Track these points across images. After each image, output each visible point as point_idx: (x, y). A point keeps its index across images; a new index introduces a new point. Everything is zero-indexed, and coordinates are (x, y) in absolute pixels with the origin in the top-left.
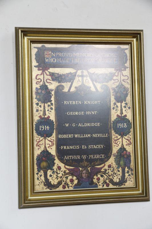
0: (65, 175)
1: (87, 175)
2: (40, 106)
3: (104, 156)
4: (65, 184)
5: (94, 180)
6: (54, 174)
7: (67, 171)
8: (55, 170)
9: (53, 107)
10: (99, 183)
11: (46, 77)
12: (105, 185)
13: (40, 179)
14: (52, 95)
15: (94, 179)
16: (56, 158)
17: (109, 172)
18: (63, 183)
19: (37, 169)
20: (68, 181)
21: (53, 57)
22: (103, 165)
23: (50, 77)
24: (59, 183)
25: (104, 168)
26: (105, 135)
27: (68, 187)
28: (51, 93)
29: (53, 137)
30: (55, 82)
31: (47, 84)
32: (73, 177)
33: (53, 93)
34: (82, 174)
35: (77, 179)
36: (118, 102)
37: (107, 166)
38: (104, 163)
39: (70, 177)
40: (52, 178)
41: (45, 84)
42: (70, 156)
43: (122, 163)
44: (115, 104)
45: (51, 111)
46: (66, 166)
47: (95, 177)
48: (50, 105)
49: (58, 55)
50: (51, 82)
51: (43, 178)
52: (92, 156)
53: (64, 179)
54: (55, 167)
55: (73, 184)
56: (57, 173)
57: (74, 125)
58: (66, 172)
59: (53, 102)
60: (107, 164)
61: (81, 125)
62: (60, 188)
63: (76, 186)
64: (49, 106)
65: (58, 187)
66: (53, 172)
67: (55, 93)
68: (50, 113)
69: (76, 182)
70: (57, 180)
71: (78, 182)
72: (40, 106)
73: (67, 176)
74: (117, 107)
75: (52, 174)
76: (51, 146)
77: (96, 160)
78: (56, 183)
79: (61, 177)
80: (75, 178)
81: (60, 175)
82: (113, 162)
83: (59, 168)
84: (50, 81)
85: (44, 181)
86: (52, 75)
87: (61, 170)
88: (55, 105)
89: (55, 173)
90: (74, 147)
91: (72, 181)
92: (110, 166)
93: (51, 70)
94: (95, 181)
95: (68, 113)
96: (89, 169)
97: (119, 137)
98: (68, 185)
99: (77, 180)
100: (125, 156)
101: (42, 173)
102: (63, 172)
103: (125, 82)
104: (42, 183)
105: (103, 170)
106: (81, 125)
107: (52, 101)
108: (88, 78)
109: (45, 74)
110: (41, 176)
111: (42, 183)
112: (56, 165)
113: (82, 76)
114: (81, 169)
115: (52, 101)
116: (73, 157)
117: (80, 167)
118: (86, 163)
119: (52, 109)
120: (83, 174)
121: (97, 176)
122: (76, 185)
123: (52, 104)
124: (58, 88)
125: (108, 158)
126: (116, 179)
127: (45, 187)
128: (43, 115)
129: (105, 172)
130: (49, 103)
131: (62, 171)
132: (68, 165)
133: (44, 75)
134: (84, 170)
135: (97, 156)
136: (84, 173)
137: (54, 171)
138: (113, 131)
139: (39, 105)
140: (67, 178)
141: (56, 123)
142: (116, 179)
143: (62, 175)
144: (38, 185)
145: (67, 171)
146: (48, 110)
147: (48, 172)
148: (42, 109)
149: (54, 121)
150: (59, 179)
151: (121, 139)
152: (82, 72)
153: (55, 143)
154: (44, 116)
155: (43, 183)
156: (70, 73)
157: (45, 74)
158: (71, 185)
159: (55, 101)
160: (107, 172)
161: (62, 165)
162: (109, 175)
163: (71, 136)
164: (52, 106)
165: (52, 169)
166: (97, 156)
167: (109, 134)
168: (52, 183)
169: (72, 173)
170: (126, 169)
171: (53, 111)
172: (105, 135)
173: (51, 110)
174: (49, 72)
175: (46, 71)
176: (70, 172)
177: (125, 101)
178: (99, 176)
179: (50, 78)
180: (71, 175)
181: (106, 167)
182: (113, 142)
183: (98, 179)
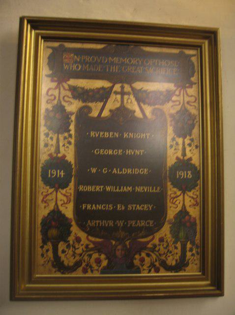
0: (87, 251)
1: (123, 252)
2: (52, 139)
3: (154, 223)
4: (87, 265)
5: (134, 261)
6: (69, 249)
7: (91, 246)
8: (71, 242)
9: (73, 141)
10: (142, 266)
11: (63, 93)
12: (153, 270)
13: (45, 256)
14: (72, 121)
15: (135, 259)
16: (73, 223)
17: (159, 250)
18: (84, 264)
19: (42, 239)
20: (92, 260)
21: (76, 62)
22: (151, 237)
23: (70, 93)
24: (78, 264)
25: (152, 243)
26: (156, 189)
27: (92, 271)
28: (70, 118)
29: (70, 189)
30: (77, 100)
31: (64, 103)
32: (100, 255)
33: (73, 118)
34: (115, 250)
35: (107, 258)
36: (179, 136)
37: (158, 239)
38: (153, 234)
39: (95, 256)
40: (66, 255)
41: (61, 102)
42: (97, 222)
43: (182, 234)
44: (173, 139)
45: (67, 147)
46: (90, 238)
47: (137, 256)
48: (68, 137)
49: (84, 60)
50: (72, 100)
51: (50, 254)
52: (133, 222)
53: (86, 258)
54: (71, 239)
55: (100, 266)
56: (74, 247)
57: (105, 171)
58: (90, 246)
59: (73, 132)
60: (158, 236)
61: (117, 171)
62: (79, 274)
63: (105, 270)
64: (65, 138)
65: (75, 270)
66: (68, 246)
67: (77, 118)
68: (67, 149)
69: (105, 263)
70: (74, 258)
71: (108, 264)
72: (52, 139)
73: (91, 252)
74: (177, 144)
75: (65, 249)
76: (67, 203)
77: (140, 229)
78: (71, 264)
79: (81, 255)
80: (103, 256)
81: (79, 251)
82: (168, 233)
83: (78, 240)
84: (70, 100)
85: (52, 259)
86: (73, 89)
87: (82, 243)
88: (75, 137)
89: (71, 248)
90: (104, 207)
91: (98, 261)
92: (161, 240)
93: (72, 82)
94: (137, 262)
95: (97, 151)
96: (127, 243)
97: (179, 193)
98: (91, 267)
99: (107, 261)
100: (188, 224)
101: (49, 246)
102: (83, 247)
103: (191, 105)
104: (48, 262)
105: (150, 246)
106: (117, 171)
107: (70, 130)
108: (132, 97)
109: (62, 88)
110: (47, 251)
111: (48, 262)
112: (73, 234)
113: (123, 93)
114: (114, 243)
115: (70, 130)
116: (102, 222)
117: (114, 240)
118: (122, 234)
119: (70, 143)
120: (116, 252)
121: (140, 255)
122: (105, 268)
123: (70, 136)
124: (81, 110)
125: (159, 226)
126: (171, 261)
127: (54, 270)
128: (55, 152)
129: (153, 249)
130: (66, 134)
131: (82, 245)
132: (93, 236)
133: (60, 89)
134: (120, 244)
135: (142, 223)
136: (118, 250)
137: (69, 244)
138: (169, 184)
139: (50, 136)
140: (90, 256)
141: (76, 166)
142: (171, 261)
143: (82, 252)
144: (43, 265)
145: (91, 246)
146: (64, 145)
147: (60, 245)
148: (54, 142)
149: (73, 162)
150: (78, 258)
151: (182, 196)
152: (122, 87)
153: (72, 198)
154: (57, 154)
155: (50, 264)
156: (103, 88)
157: (62, 88)
158: (96, 268)
159: (76, 131)
160: (157, 249)
161: (83, 235)
162: (160, 255)
163: (100, 189)
164: (70, 139)
165: (66, 241)
166: (142, 223)
167: (162, 187)
168: (66, 263)
169: (98, 248)
170: (189, 246)
171: (72, 147)
172: (156, 189)
173: (68, 145)
174: (69, 85)
175: (64, 84)
176: (96, 247)
177: (190, 136)
178: (143, 255)
179: (69, 94)
180: (97, 252)
181: (156, 241)
182: (168, 201)
183: (142, 260)
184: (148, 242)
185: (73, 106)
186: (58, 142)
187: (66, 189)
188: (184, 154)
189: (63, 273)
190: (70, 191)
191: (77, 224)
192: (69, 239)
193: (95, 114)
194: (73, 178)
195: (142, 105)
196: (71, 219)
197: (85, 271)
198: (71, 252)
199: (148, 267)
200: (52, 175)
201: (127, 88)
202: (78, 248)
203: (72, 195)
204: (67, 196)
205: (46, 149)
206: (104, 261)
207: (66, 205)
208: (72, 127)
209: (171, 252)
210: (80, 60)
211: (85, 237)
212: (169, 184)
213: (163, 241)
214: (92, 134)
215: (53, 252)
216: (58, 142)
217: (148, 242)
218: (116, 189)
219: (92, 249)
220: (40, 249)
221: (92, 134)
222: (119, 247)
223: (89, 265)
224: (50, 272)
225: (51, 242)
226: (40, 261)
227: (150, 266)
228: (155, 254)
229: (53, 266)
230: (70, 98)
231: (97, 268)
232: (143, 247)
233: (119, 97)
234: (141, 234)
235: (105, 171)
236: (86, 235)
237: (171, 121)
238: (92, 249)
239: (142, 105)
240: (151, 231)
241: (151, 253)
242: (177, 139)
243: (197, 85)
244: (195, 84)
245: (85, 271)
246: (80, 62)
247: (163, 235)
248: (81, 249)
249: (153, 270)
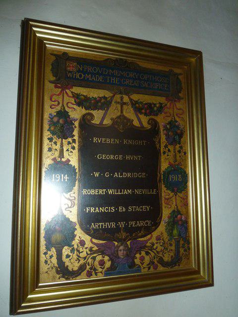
0: (91, 254)
1: (125, 252)
2: (56, 143)
3: (151, 223)
4: (91, 268)
5: (135, 260)
6: (74, 253)
7: (95, 248)
8: (75, 246)
9: (76, 145)
10: (142, 264)
11: (66, 99)
12: (152, 267)
13: (49, 262)
14: (75, 127)
15: (136, 258)
16: (77, 227)
17: (157, 248)
18: (88, 267)
19: (46, 245)
20: (96, 263)
21: (79, 71)
22: (149, 236)
23: (73, 100)
24: (82, 268)
25: (150, 241)
26: (153, 191)
27: (96, 274)
28: (74, 124)
29: (74, 193)
30: (81, 107)
31: (67, 109)
32: (104, 257)
33: (77, 124)
34: (117, 251)
35: (111, 259)
36: (171, 144)
37: (155, 238)
38: (151, 233)
39: (99, 258)
40: (70, 260)
41: (64, 108)
42: (100, 224)
43: (175, 232)
44: (166, 146)
45: (71, 152)
46: (94, 240)
47: (138, 256)
48: (71, 142)
49: (87, 70)
50: (75, 107)
51: (54, 260)
52: (133, 223)
53: (90, 261)
54: (75, 242)
55: (104, 268)
56: (78, 251)
57: (107, 174)
58: (93, 249)
59: (76, 138)
60: (155, 234)
61: (118, 176)
62: (83, 278)
63: (109, 271)
64: (69, 143)
65: (80, 274)
66: (72, 251)
67: (81, 125)
68: (71, 154)
69: (108, 264)
70: (79, 262)
71: (112, 265)
72: (56, 143)
73: (95, 255)
74: (169, 151)
75: (70, 254)
76: (70, 207)
77: (139, 229)
78: (76, 269)
79: (85, 258)
80: (106, 258)
81: (83, 255)
82: (164, 232)
83: (82, 243)
84: (72, 106)
85: (56, 265)
86: (76, 96)
87: (86, 246)
88: (79, 142)
89: (76, 252)
90: (107, 209)
91: (102, 263)
92: (158, 238)
93: (76, 90)
94: (137, 261)
95: (99, 157)
96: (129, 243)
97: (172, 194)
98: (95, 269)
99: (110, 262)
100: (180, 222)
101: (53, 251)
102: (88, 250)
103: (179, 117)
104: (52, 268)
105: (148, 244)
106: (118, 176)
107: (74, 136)
108: (130, 106)
109: (65, 95)
110: (51, 257)
111: (52, 268)
112: (77, 238)
113: (123, 104)
114: (116, 243)
115: (74, 136)
116: (105, 224)
117: (116, 241)
118: (124, 235)
119: (73, 148)
120: (119, 252)
121: (140, 254)
122: (108, 269)
123: (74, 141)
124: (84, 117)
125: (157, 225)
126: (167, 258)
127: (58, 276)
128: (59, 157)
129: (151, 248)
130: (70, 140)
131: (86, 248)
132: (96, 239)
133: (63, 96)
134: (122, 245)
135: (140, 224)
136: (121, 250)
137: (73, 249)
138: (163, 186)
139: (54, 141)
140: (94, 258)
141: (79, 171)
142: (167, 258)
143: (86, 255)
144: (47, 272)
145: (95, 248)
146: (68, 150)
147: (64, 250)
148: (58, 147)
149: (77, 167)
150: (82, 262)
151: (174, 197)
152: (122, 98)
153: (76, 202)
154: (61, 159)
155: (54, 270)
156: (105, 98)
157: (65, 95)
158: (100, 270)
159: (79, 137)
160: (155, 247)
161: (87, 238)
162: (158, 252)
163: (103, 192)
164: (74, 144)
165: (70, 245)
166: (140, 224)
167: (157, 190)
168: (70, 269)
169: (102, 251)
170: (181, 242)
171: (76, 152)
172: (153, 191)
173: (72, 150)
174: (72, 92)
175: (68, 91)
176: (99, 249)
177: (180, 144)
178: (143, 253)
179: (73, 100)
180: (101, 255)
181: (154, 240)
182: (163, 202)
183: (142, 259)
184: (146, 242)
185: (76, 113)
186: (62, 146)
187: (70, 193)
188: (176, 160)
189: (67, 279)
190: (74, 195)
191: (82, 228)
192: (73, 243)
193: (96, 121)
194: (77, 182)
195: (139, 115)
196: (75, 223)
197: (89, 274)
198: (75, 256)
199: (147, 265)
200: (172, 179)
201: (126, 99)
202: (82, 252)
203: (76, 199)
204: (71, 200)
205: (50, 153)
206: (107, 263)
207: (70, 209)
208: (76, 133)
209: (167, 249)
210: (83, 69)
211: (89, 240)
212: (163, 186)
213: (160, 239)
214: (95, 140)
215: (57, 258)
216: (62, 146)
217: (146, 242)
218: (117, 192)
219: (95, 252)
220: (44, 256)
221: (95, 140)
222: (121, 248)
223: (93, 269)
224: (54, 279)
225: (55, 247)
226: (43, 268)
227: (149, 264)
228: (153, 252)
229: (58, 272)
230: (74, 104)
231: (102, 270)
232: (143, 247)
233: (119, 106)
234: (140, 234)
235: (107, 175)
236: (89, 238)
237: (164, 130)
238: (95, 252)
239: (139, 115)
240: (148, 231)
241: (150, 251)
242: (169, 147)
243: (184, 99)
244: (183, 98)
245: (89, 274)
246: (82, 72)
247: (159, 234)
248: (85, 252)
249: (152, 267)
